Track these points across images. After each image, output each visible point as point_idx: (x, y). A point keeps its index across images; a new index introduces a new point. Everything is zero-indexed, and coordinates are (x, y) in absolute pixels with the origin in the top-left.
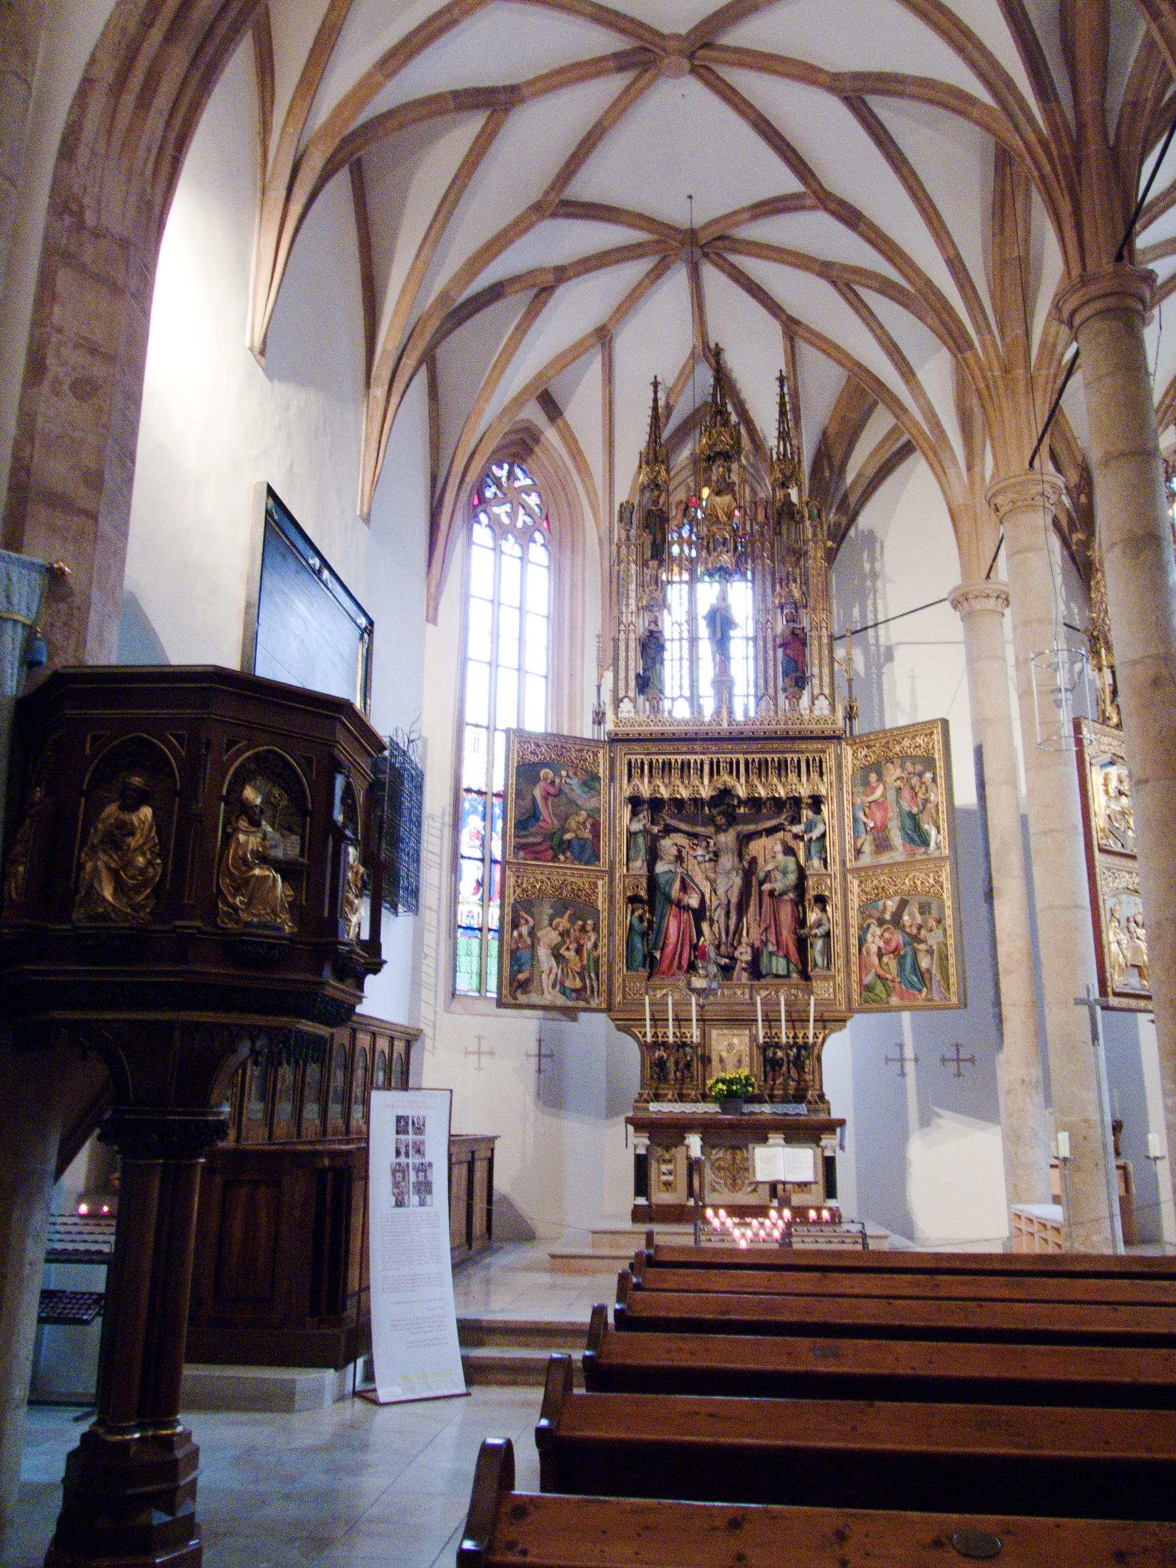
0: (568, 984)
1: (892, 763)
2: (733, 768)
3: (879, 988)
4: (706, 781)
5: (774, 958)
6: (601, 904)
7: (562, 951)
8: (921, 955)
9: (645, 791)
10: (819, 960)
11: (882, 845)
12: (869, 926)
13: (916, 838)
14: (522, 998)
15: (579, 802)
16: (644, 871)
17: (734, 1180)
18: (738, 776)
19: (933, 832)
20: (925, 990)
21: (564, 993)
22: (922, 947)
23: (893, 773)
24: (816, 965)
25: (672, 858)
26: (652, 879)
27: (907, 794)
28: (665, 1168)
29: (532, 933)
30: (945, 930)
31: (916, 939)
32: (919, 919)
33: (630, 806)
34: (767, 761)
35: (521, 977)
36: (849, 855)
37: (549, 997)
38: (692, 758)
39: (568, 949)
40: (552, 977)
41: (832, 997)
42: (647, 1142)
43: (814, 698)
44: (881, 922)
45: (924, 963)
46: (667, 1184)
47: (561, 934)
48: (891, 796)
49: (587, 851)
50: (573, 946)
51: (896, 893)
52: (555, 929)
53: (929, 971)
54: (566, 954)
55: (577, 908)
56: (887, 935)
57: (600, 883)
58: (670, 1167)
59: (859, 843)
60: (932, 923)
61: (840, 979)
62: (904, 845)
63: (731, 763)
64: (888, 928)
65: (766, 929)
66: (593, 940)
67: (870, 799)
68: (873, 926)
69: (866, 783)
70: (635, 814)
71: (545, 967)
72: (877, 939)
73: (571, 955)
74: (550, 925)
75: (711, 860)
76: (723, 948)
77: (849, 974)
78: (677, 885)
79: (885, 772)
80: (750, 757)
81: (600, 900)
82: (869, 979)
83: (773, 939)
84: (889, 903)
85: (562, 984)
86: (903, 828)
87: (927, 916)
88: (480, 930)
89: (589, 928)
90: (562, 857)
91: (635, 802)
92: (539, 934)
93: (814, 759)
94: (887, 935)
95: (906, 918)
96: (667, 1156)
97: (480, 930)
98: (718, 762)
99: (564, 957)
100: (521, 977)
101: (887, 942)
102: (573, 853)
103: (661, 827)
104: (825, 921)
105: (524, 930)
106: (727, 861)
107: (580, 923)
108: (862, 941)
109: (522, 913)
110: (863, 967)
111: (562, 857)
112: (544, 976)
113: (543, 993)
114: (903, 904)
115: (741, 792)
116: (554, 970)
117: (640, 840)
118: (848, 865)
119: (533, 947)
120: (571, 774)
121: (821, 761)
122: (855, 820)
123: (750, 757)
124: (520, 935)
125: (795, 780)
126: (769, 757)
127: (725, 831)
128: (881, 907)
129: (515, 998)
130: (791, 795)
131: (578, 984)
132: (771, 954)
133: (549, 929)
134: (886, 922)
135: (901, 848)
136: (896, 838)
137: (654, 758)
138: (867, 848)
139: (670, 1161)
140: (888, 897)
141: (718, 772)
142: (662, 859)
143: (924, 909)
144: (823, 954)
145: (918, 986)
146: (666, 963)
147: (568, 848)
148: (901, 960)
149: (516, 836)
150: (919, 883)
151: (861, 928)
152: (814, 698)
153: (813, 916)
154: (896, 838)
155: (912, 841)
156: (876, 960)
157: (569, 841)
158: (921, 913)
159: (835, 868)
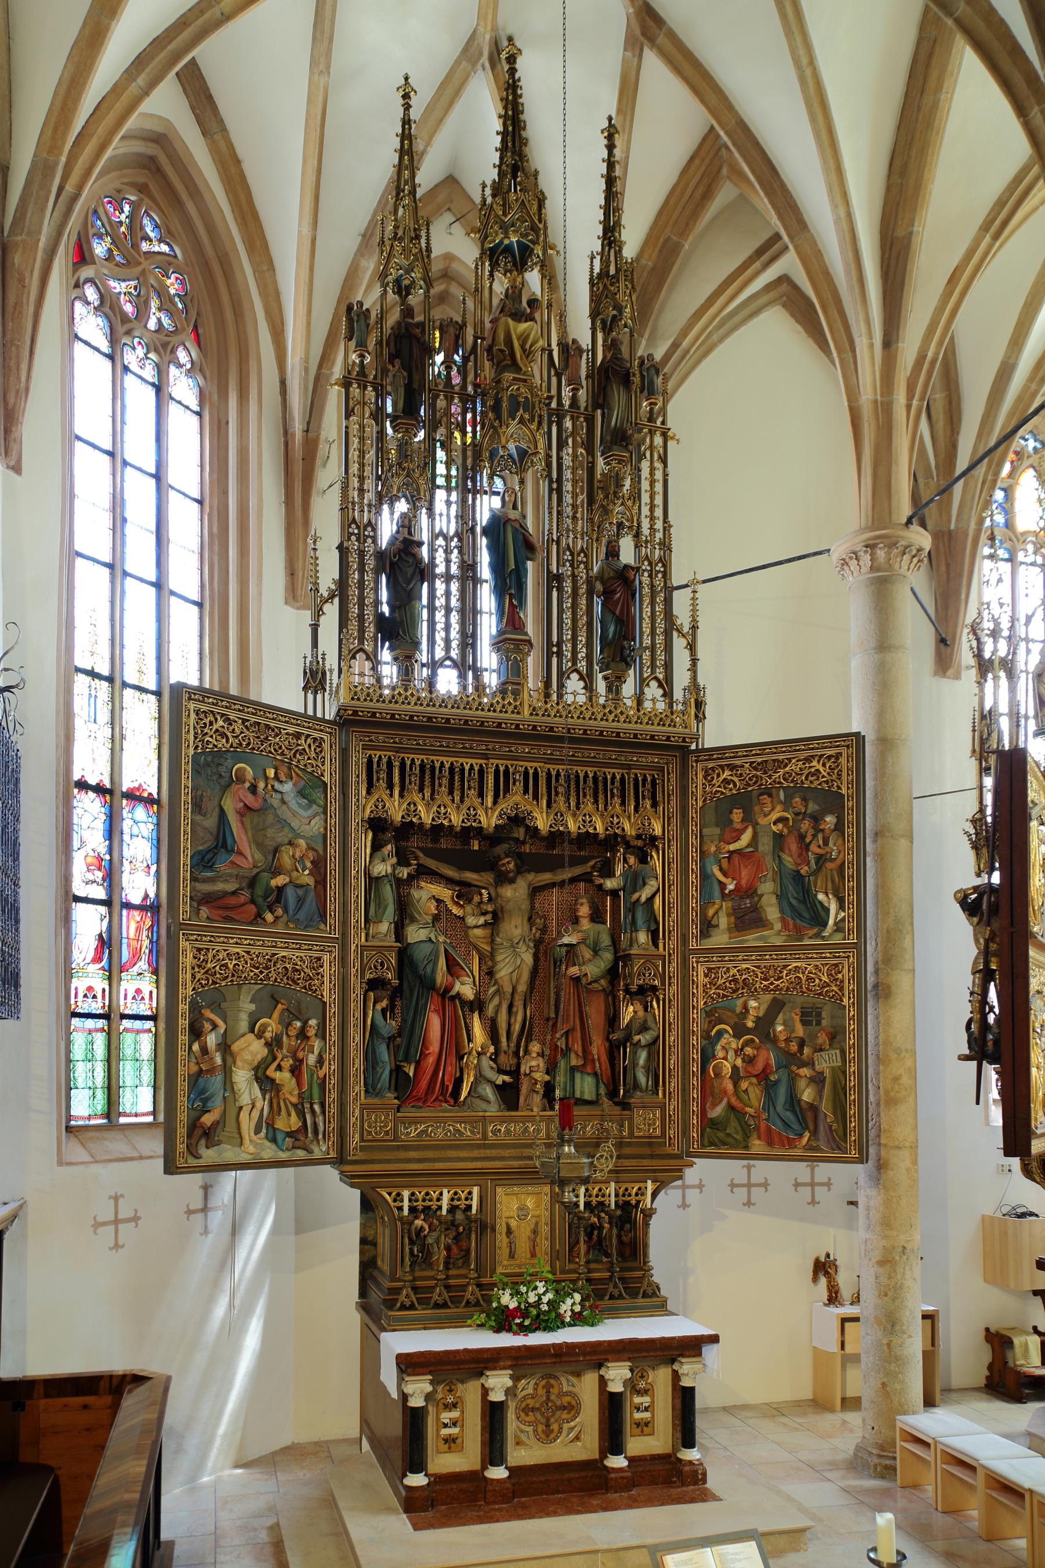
0: (280, 1124)
1: (770, 795)
2: (530, 783)
3: (733, 1127)
4: (489, 800)
5: (578, 1076)
6: (328, 992)
7: (271, 1072)
8: (802, 1083)
9: (396, 810)
10: (642, 1079)
11: (748, 918)
12: (720, 1034)
13: (806, 915)
14: (209, 1155)
15: (295, 824)
16: (391, 941)
17: (548, 1425)
18: (536, 797)
19: (833, 907)
20: (807, 1135)
21: (274, 1140)
22: (805, 1071)
23: (771, 816)
24: (636, 1086)
25: (429, 919)
26: (405, 954)
27: (793, 845)
28: (446, 1416)
29: (225, 1047)
30: (843, 1053)
31: (791, 1060)
32: (800, 1031)
33: (370, 835)
34: (577, 776)
35: (207, 1119)
36: (694, 930)
37: (252, 1149)
38: (467, 762)
39: (279, 1068)
40: (256, 1114)
41: (658, 1132)
42: (429, 1388)
43: (642, 683)
44: (739, 1031)
45: (807, 1095)
46: (450, 1441)
47: (267, 1044)
48: (766, 845)
49: (311, 908)
50: (287, 1063)
51: (766, 989)
52: (259, 1036)
53: (814, 1108)
54: (277, 1076)
55: (287, 997)
56: (749, 1051)
57: (326, 958)
58: (455, 1414)
59: (711, 912)
60: (822, 1038)
61: (673, 1106)
62: (783, 920)
63: (526, 773)
64: (752, 1041)
65: (567, 1033)
66: (316, 1052)
67: (732, 847)
68: (726, 1036)
69: (724, 822)
70: (376, 847)
71: (245, 1100)
72: (731, 1054)
73: (283, 1077)
74: (252, 1030)
75: (486, 925)
76: (502, 1059)
77: (685, 1102)
78: (442, 962)
79: (757, 809)
80: (554, 768)
81: (326, 986)
82: (717, 1112)
83: (578, 1047)
84: (753, 1004)
85: (271, 1125)
86: (781, 897)
87: (814, 1028)
88: (106, 1016)
89: (311, 1032)
90: (269, 917)
91: (378, 825)
92: (235, 1047)
93: (645, 780)
94: (749, 1051)
95: (779, 1028)
96: (450, 1399)
97: (106, 1016)
98: (507, 771)
99: (273, 1081)
100: (207, 1119)
101: (750, 1061)
102: (286, 910)
103: (411, 869)
104: (650, 1023)
105: (212, 1040)
106: (515, 927)
107: (299, 1024)
108: (707, 1057)
109: (208, 1014)
110: (708, 1092)
111: (269, 917)
112: (244, 1116)
113: (241, 1144)
114: (776, 1007)
115: (542, 822)
116: (259, 1104)
117: (388, 892)
118: (693, 945)
119: (227, 1072)
120: (283, 778)
121: (654, 781)
122: (705, 877)
123: (554, 768)
124: (204, 1050)
125: (618, 809)
126: (581, 770)
127: (512, 881)
128: (738, 1010)
129: (198, 1157)
130: (611, 832)
131: (295, 1122)
132: (573, 1069)
133: (251, 1036)
134: (749, 1031)
135: (778, 926)
136: (772, 912)
137: (408, 758)
138: (723, 921)
139: (455, 1405)
140: (754, 994)
141: (507, 790)
142: (413, 920)
143: (810, 1016)
144: (648, 1072)
145: (796, 1126)
146: (424, 1083)
147: (278, 900)
148: (769, 1088)
149: (194, 879)
150: (804, 979)
151: (706, 1035)
152: (642, 683)
153: (628, 1012)
154: (772, 912)
155: (796, 913)
156: (729, 1086)
157: (280, 889)
158: (804, 1023)
159: (670, 944)
